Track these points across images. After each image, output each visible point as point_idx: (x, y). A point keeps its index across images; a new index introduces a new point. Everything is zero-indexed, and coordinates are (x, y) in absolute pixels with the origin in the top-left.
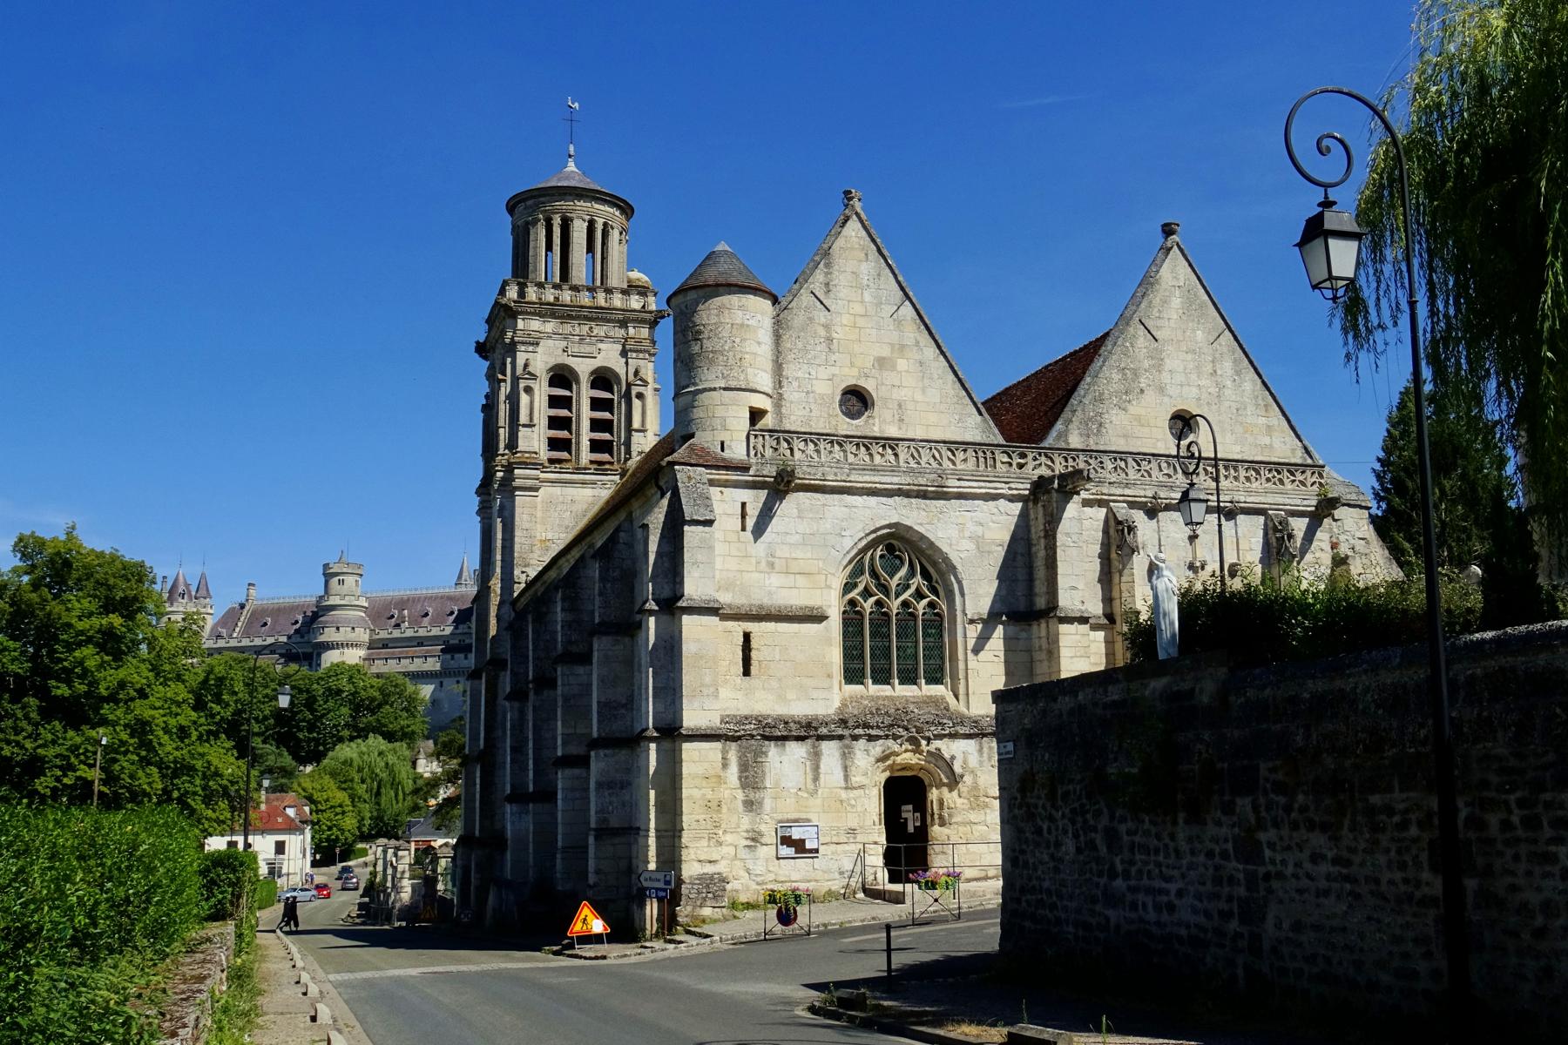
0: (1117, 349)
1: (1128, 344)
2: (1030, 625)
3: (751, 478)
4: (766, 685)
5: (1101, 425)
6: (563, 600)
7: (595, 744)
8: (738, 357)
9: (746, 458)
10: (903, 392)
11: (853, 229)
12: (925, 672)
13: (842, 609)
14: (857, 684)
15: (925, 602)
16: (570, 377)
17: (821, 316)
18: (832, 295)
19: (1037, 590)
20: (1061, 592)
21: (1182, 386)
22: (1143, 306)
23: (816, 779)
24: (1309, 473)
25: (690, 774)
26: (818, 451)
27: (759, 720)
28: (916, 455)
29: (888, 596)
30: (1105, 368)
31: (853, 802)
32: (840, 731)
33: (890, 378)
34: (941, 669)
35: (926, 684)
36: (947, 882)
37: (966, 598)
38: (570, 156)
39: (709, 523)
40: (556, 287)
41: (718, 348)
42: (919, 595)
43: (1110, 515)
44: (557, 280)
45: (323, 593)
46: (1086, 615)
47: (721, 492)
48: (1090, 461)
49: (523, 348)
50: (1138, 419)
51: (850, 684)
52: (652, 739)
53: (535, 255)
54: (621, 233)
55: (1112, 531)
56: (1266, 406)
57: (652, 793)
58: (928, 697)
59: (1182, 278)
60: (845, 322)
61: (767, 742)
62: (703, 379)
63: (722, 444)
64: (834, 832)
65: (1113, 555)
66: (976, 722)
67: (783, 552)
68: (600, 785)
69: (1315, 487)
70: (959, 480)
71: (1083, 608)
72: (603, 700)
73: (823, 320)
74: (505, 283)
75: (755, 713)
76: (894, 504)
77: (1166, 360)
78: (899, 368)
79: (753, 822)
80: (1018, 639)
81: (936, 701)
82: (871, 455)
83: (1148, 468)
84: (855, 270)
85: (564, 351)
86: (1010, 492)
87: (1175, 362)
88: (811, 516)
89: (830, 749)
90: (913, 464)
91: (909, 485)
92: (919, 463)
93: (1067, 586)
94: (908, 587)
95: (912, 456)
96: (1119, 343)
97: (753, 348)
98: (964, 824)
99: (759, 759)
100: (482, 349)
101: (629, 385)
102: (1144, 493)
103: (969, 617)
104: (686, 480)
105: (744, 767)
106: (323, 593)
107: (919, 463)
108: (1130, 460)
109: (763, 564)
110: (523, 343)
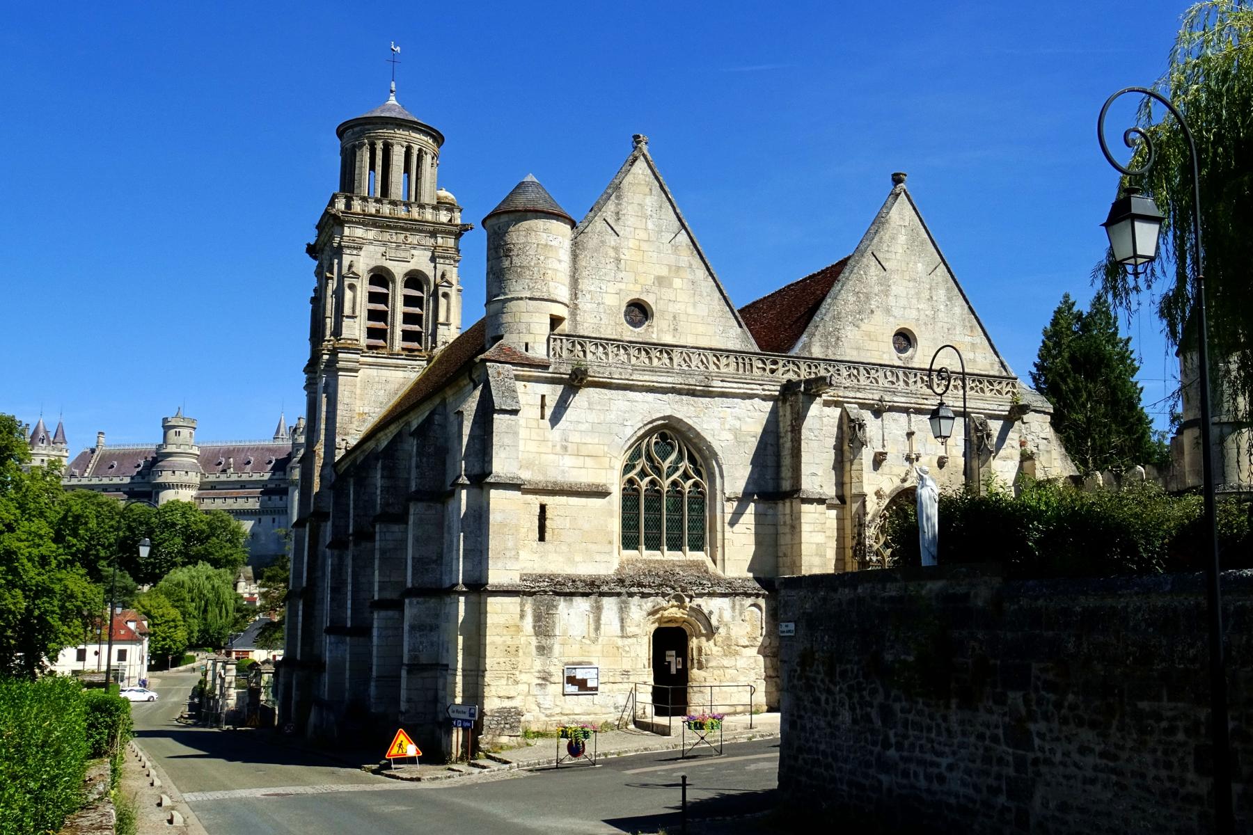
0: (853, 276)
1: (862, 272)
2: (777, 504)
3: (550, 375)
4: (558, 549)
5: (838, 339)
6: (383, 469)
7: (410, 593)
8: (542, 272)
9: (546, 357)
10: (678, 306)
11: (640, 168)
12: (689, 541)
13: (622, 487)
14: (633, 549)
15: (690, 482)
16: (387, 278)
17: (612, 240)
18: (621, 222)
19: (783, 475)
20: (804, 478)
21: (905, 308)
22: (875, 241)
23: (597, 628)
24: (1004, 384)
25: (493, 624)
26: (606, 354)
27: (551, 578)
28: (687, 359)
29: (660, 476)
30: (842, 292)
31: (627, 649)
32: (618, 590)
33: (667, 294)
34: (702, 538)
35: (690, 550)
36: (712, 723)
37: (725, 479)
38: (392, 92)
39: (515, 412)
40: (377, 201)
41: (525, 263)
42: (686, 476)
43: (844, 414)
44: (378, 195)
45: (162, 443)
46: (824, 497)
47: (525, 386)
48: (829, 368)
49: (348, 252)
50: (868, 334)
51: (627, 549)
52: (461, 593)
53: (361, 174)
54: (433, 158)
55: (845, 428)
56: (971, 327)
57: (460, 639)
58: (691, 561)
59: (907, 218)
60: (631, 246)
61: (557, 598)
62: (512, 289)
63: (527, 345)
64: (611, 674)
65: (846, 447)
66: (730, 583)
67: (575, 438)
68: (412, 628)
69: (1009, 395)
70: (722, 381)
71: (821, 491)
72: (417, 556)
73: (613, 243)
74: (334, 197)
75: (548, 572)
76: (667, 400)
77: (892, 287)
78: (675, 286)
79: (544, 664)
80: (766, 515)
81: (698, 565)
82: (650, 358)
83: (875, 376)
84: (641, 203)
85: (383, 255)
86: (764, 393)
87: (900, 287)
88: (599, 408)
89: (610, 604)
90: (685, 367)
91: (681, 384)
92: (689, 366)
93: (808, 473)
94: (677, 469)
95: (684, 360)
96: (855, 271)
97: (556, 265)
98: (718, 668)
99: (551, 612)
100: (312, 250)
101: (436, 286)
102: (872, 396)
103: (727, 495)
104: (496, 375)
105: (538, 618)
106: (162, 443)
107: (689, 366)
108: (861, 369)
109: (558, 448)
110: (348, 247)
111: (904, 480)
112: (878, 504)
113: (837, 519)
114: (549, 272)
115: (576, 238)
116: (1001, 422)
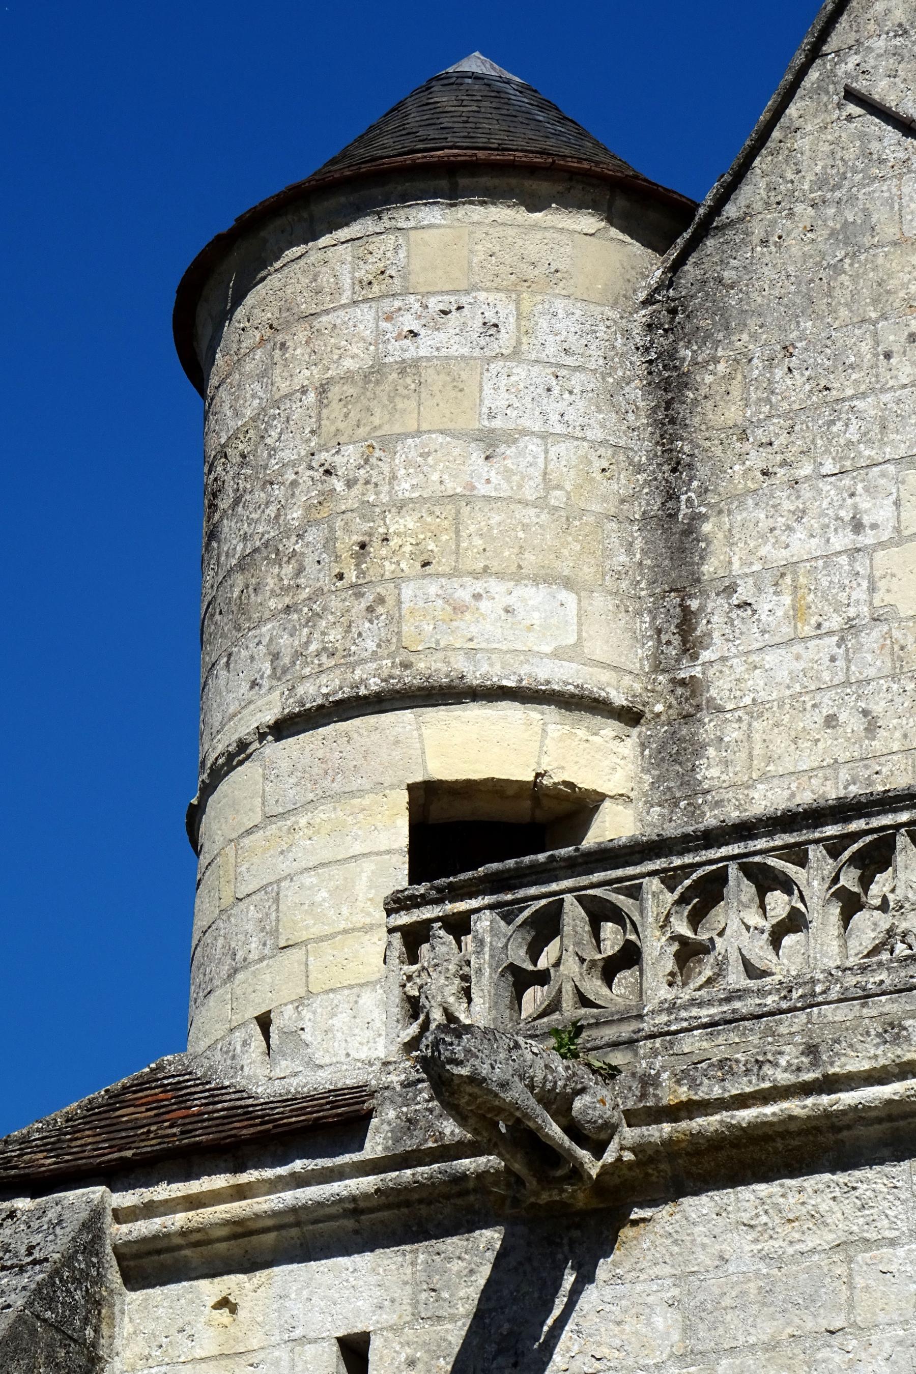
3: (367, 1183)
8: (347, 542)
47: (224, 1303)
88: (765, 1330)
114: (397, 524)
115: (668, 283)
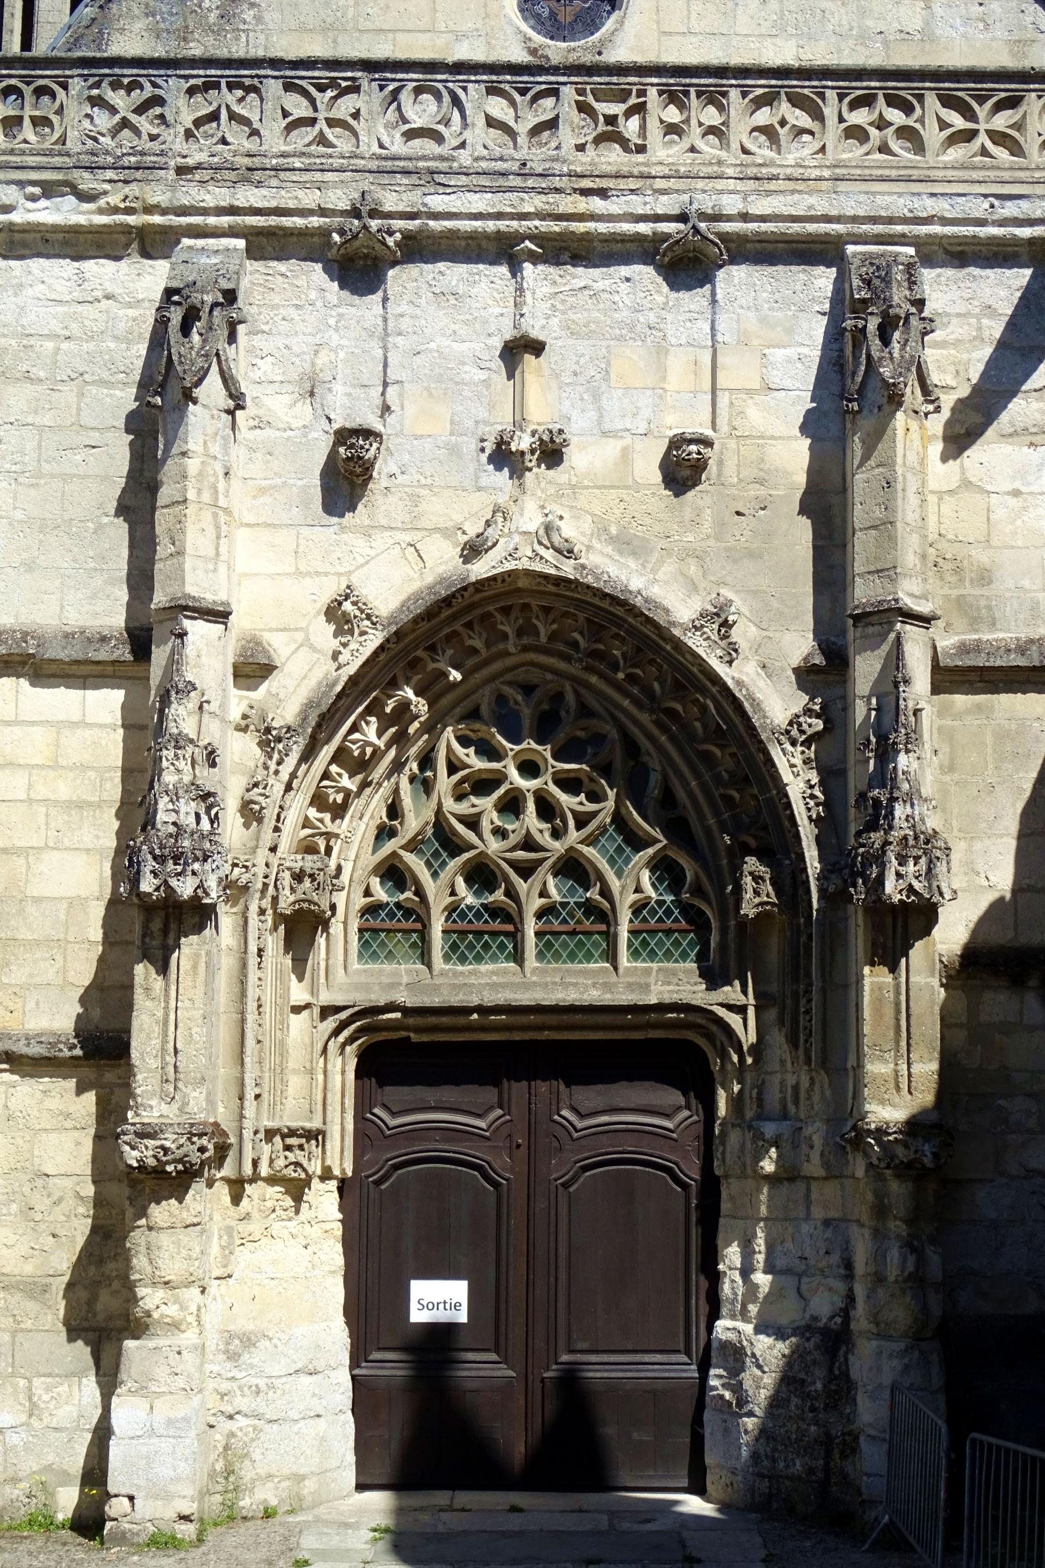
111: (473, 550)
112: (335, 656)
113: (123, 726)
116: (1022, 276)
